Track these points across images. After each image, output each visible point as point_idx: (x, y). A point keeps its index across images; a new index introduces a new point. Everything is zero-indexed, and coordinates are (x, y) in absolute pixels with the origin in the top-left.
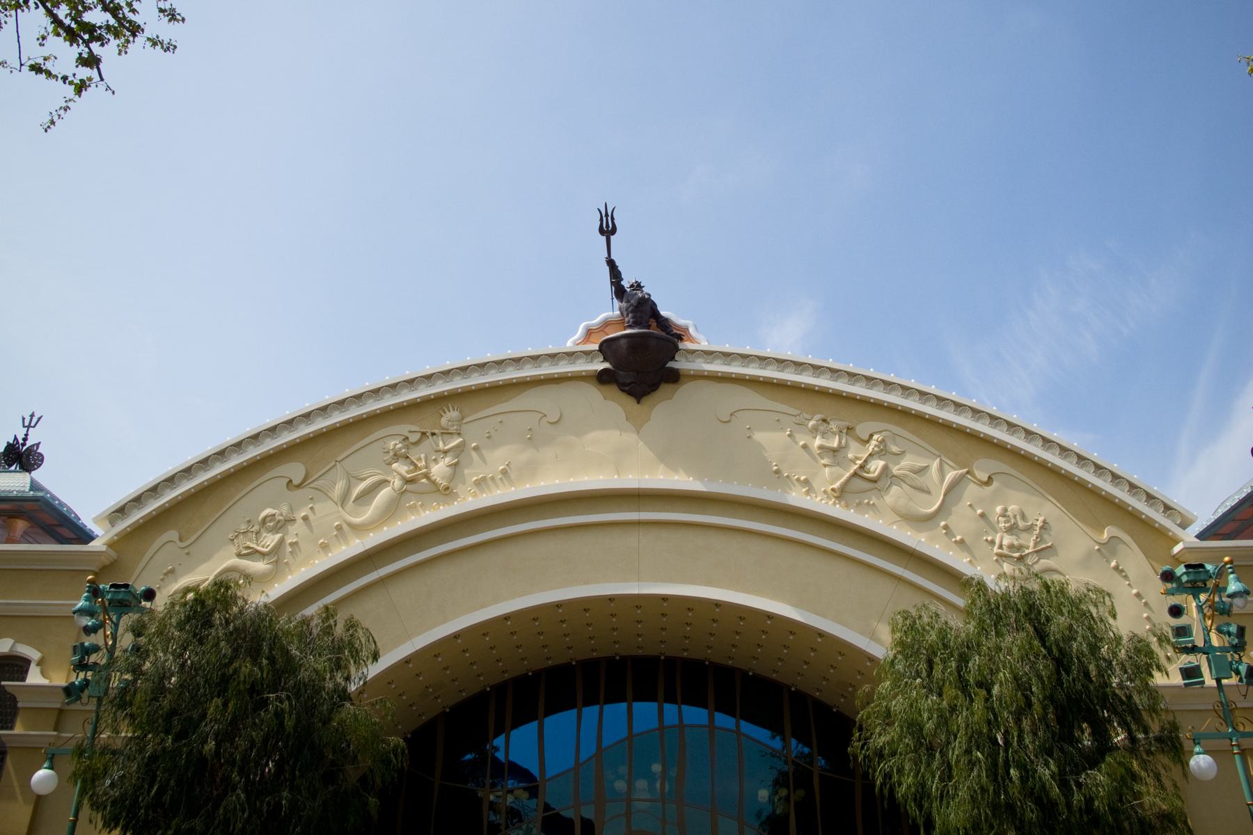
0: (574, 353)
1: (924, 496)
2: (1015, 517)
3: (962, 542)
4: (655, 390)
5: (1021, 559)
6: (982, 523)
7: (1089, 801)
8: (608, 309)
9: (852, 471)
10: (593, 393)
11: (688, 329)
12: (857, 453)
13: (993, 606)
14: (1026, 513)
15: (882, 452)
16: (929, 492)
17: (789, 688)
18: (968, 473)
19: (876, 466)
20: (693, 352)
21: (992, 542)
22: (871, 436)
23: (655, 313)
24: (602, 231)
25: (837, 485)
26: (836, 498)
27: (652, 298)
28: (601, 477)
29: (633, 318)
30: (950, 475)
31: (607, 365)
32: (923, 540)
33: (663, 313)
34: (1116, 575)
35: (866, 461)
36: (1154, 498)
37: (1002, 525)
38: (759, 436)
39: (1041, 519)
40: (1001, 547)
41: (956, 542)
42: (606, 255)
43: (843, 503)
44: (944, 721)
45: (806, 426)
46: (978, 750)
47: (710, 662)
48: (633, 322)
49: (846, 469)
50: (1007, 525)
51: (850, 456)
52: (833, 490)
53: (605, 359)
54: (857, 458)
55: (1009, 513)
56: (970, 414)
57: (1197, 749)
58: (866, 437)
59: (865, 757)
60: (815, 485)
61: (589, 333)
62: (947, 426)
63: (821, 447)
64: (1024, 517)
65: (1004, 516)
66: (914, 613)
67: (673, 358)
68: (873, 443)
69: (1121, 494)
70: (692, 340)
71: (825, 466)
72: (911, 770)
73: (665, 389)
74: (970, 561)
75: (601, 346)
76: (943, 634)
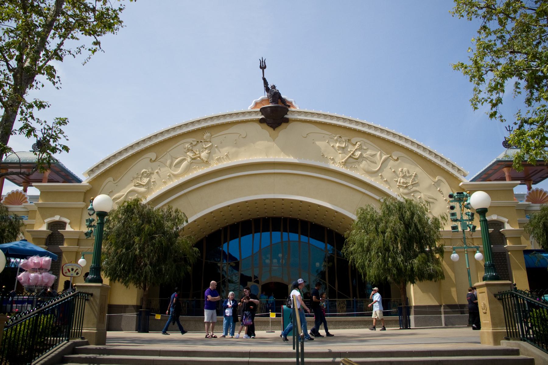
0: (251, 112)
1: (374, 164)
2: (405, 172)
3: (386, 181)
4: (279, 126)
5: (406, 187)
6: (394, 174)
7: (412, 268)
8: (264, 95)
9: (349, 155)
10: (258, 126)
11: (292, 103)
12: (351, 149)
13: (388, 207)
14: (410, 171)
15: (360, 148)
16: (376, 163)
17: (327, 228)
18: (390, 156)
19: (358, 154)
20: (294, 111)
21: (397, 181)
22: (357, 143)
23: (280, 97)
24: (261, 67)
25: (343, 161)
26: (343, 165)
27: (279, 91)
28: (261, 157)
29: (272, 99)
30: (384, 157)
31: (263, 117)
32: (373, 180)
33: (283, 96)
34: (439, 193)
35: (354, 152)
36: (455, 166)
37: (401, 175)
38: (318, 143)
39: (415, 173)
40: (400, 183)
41: (384, 181)
42: (262, 76)
43: (345, 167)
44: (370, 243)
45: (334, 139)
46: (380, 252)
47: (299, 219)
48: (272, 101)
49: (347, 155)
50: (402, 175)
51: (349, 150)
52: (342, 162)
53: (262, 114)
54: (351, 151)
55: (404, 171)
56: (392, 135)
57: (454, 252)
58: (355, 143)
59: (346, 254)
60: (336, 160)
61: (256, 104)
62: (384, 139)
63: (339, 147)
64: (409, 172)
65: (401, 172)
66: (365, 208)
67: (286, 114)
68: (357, 145)
69: (443, 165)
70: (293, 107)
71: (340, 153)
72: (360, 258)
73: (284, 125)
74: (389, 188)
75: (261, 109)
76: (372, 216)
